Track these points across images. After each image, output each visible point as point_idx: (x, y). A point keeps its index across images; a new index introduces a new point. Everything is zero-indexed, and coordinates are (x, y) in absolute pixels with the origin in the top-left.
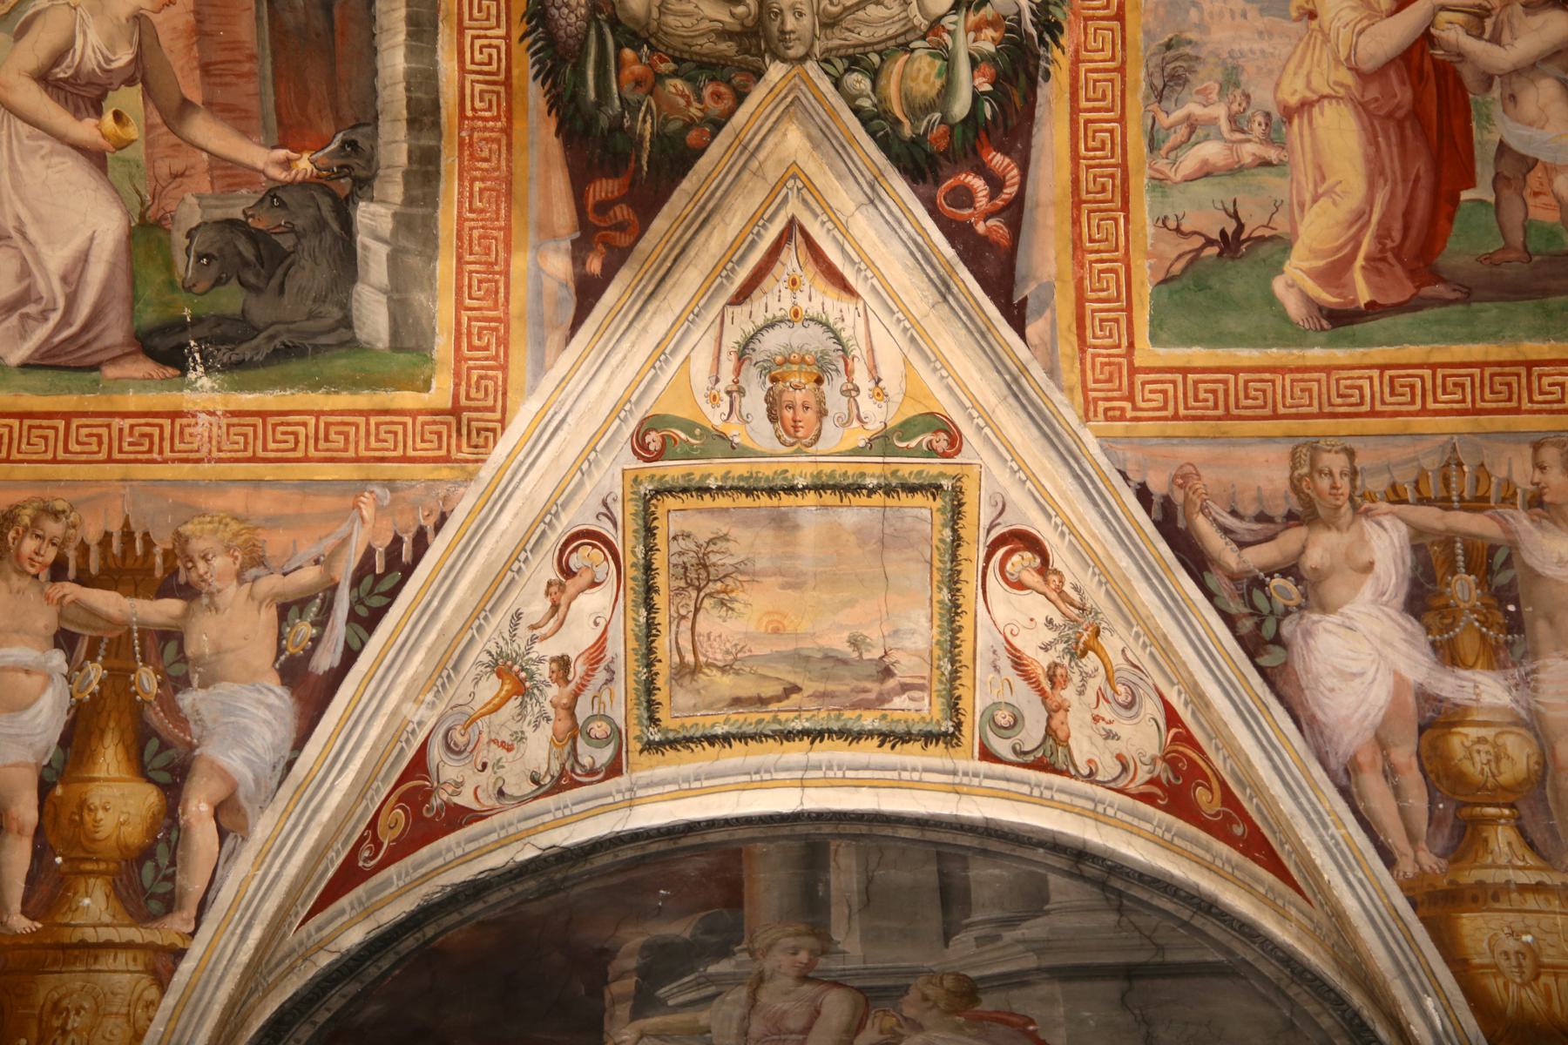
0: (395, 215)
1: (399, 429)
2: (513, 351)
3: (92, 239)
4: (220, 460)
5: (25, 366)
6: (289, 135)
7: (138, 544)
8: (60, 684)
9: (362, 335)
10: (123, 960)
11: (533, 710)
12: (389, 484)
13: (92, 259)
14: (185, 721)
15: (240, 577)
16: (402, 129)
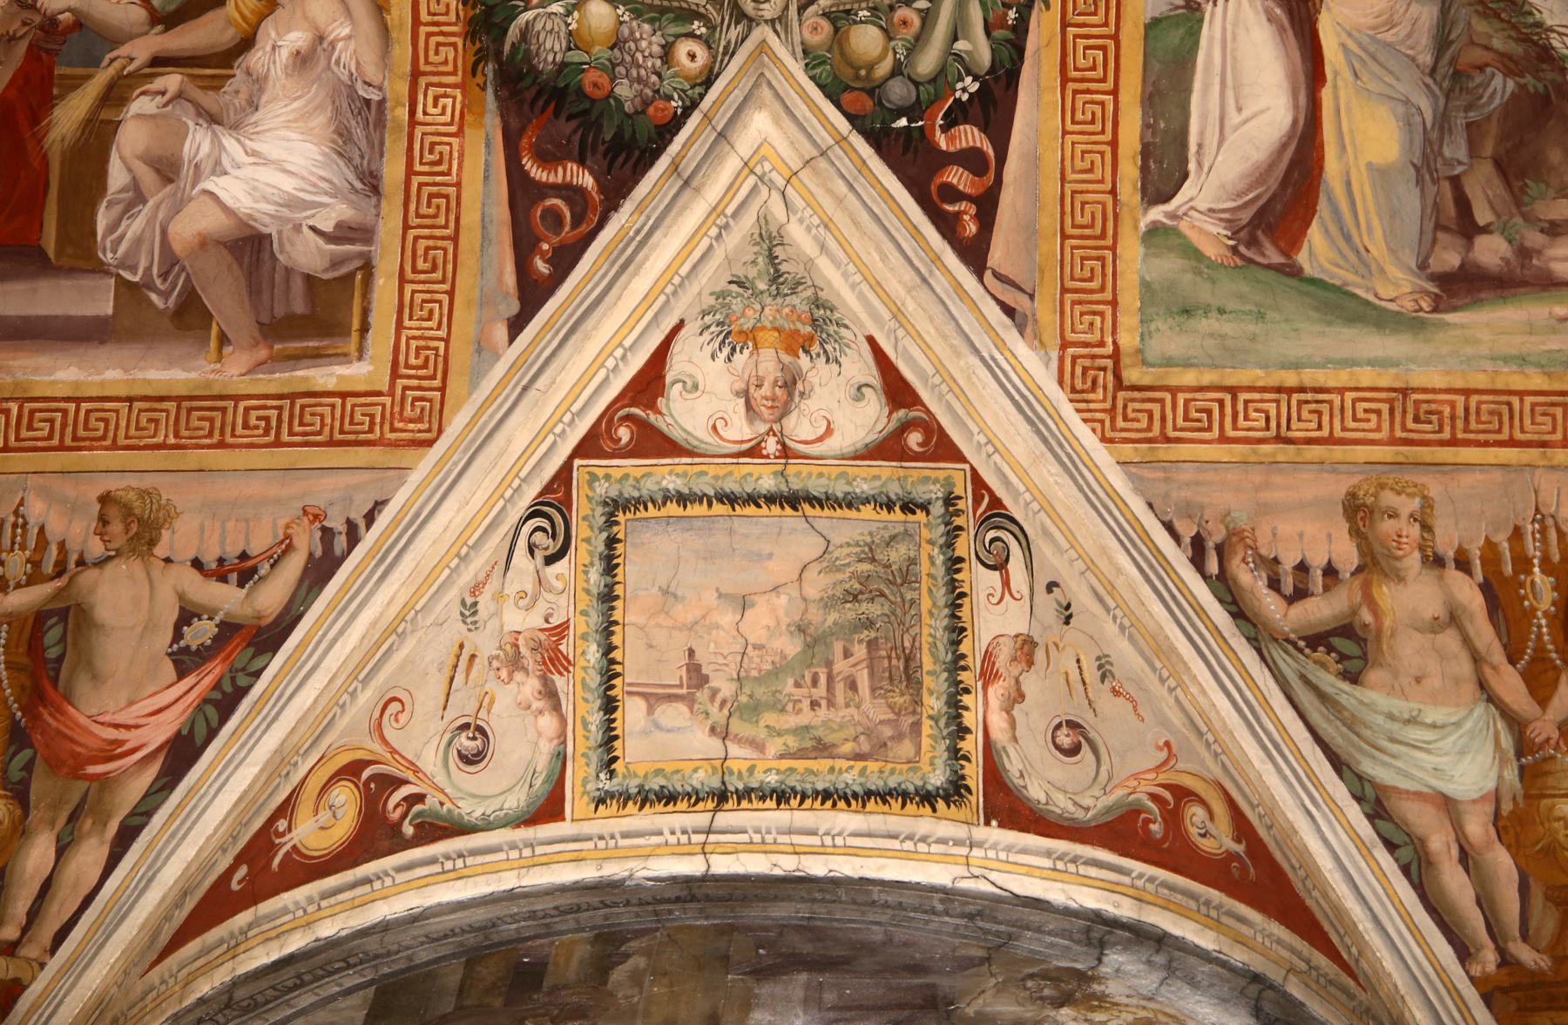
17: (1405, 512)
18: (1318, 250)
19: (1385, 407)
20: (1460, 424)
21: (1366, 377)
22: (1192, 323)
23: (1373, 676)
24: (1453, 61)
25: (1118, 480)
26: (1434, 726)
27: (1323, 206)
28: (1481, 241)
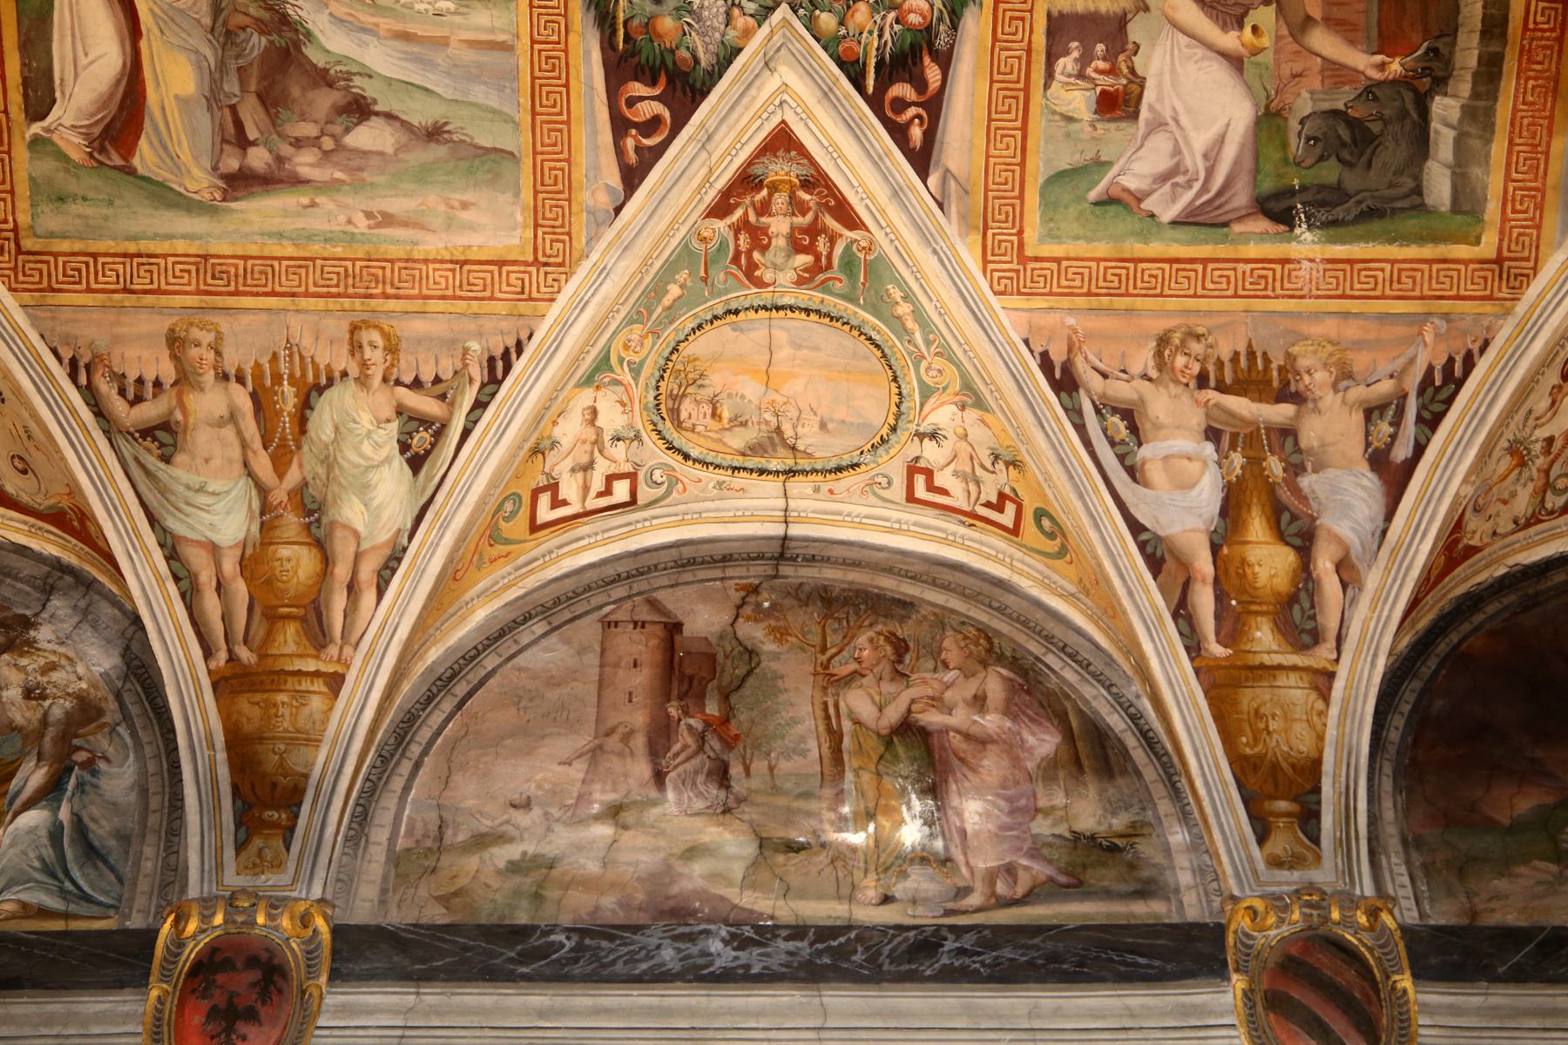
0: (1463, 107)
1: (1455, 274)
2: (1546, 213)
3: (1228, 125)
4: (1318, 297)
5: (1175, 223)
6: (1386, 44)
7: (1259, 361)
8: (1214, 468)
9: (1429, 201)
10: (1293, 679)
11: (1525, 475)
12: (1446, 316)
13: (1227, 140)
14: (1306, 498)
15: (1335, 387)
16: (1476, 38)
17: (205, 343)
18: (145, 156)
19: (193, 268)
20: (241, 280)
21: (181, 246)
22: (65, 207)
23: (180, 458)
24: (225, 23)
25: (20, 318)
26: (214, 494)
27: (147, 124)
28: (252, 151)
